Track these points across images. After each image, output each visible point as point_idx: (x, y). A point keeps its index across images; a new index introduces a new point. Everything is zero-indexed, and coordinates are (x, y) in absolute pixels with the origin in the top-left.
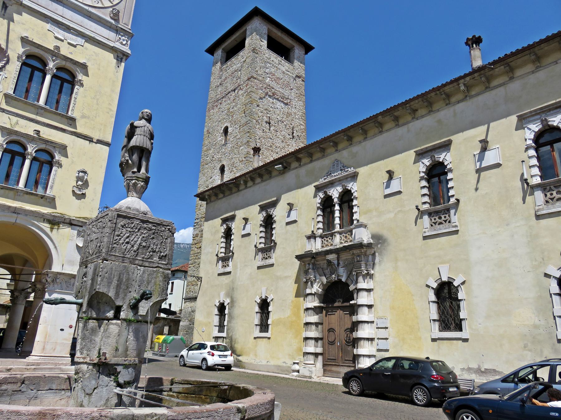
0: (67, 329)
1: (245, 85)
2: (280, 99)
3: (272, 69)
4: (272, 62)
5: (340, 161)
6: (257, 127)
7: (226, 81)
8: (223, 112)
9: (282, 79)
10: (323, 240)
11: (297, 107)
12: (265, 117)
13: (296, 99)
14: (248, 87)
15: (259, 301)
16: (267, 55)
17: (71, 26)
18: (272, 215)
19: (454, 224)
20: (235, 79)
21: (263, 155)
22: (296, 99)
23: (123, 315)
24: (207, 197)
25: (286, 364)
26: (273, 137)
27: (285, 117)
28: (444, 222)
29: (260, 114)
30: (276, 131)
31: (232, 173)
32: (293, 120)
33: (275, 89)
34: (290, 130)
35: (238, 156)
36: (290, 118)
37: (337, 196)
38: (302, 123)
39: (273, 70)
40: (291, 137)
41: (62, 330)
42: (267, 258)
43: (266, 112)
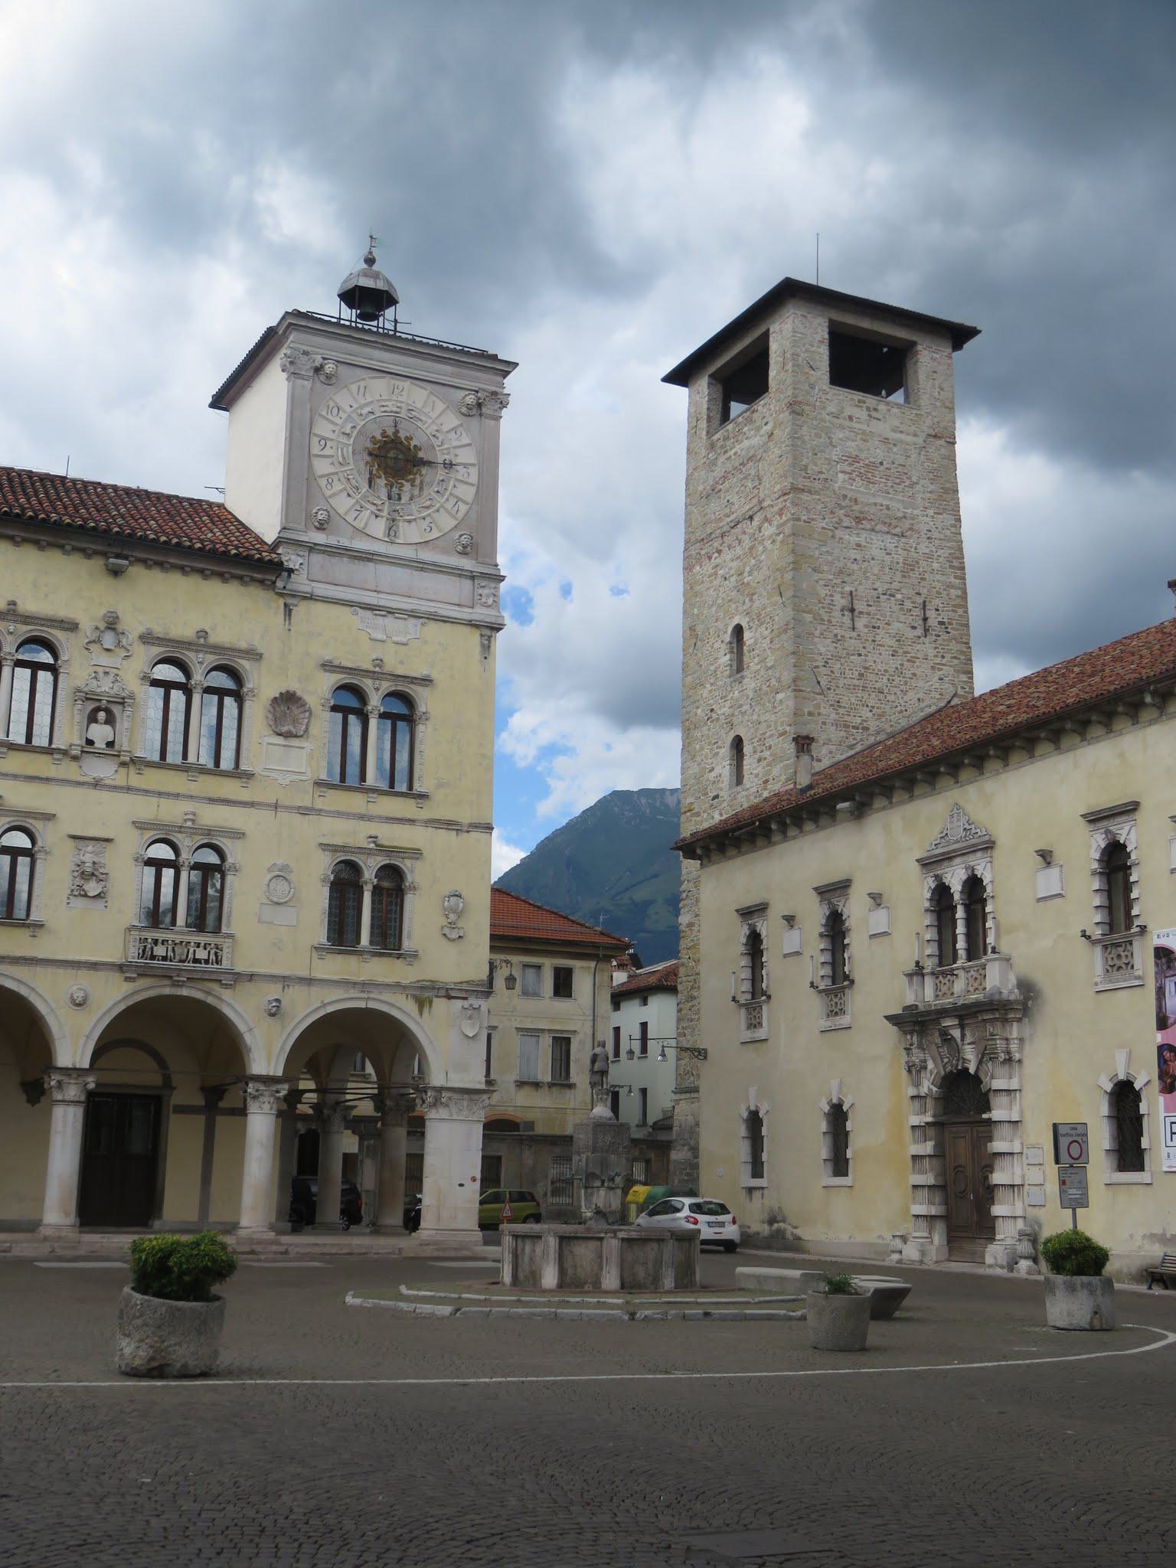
0: (468, 1184)
1: (776, 509)
2: (879, 527)
3: (849, 443)
4: (847, 423)
5: (963, 810)
6: (817, 633)
7: (727, 485)
8: (725, 579)
9: (881, 463)
10: (937, 981)
11: (935, 534)
12: (837, 597)
13: (931, 512)
14: (784, 518)
15: (826, 1108)
16: (831, 408)
17: (394, 605)
18: (841, 915)
19: (1137, 973)
20: (750, 485)
21: (840, 707)
22: (931, 512)
23: (606, 1184)
24: (699, 851)
25: (883, 1239)
26: (864, 648)
27: (898, 577)
28: (1124, 966)
29: (823, 592)
30: (874, 627)
31: (763, 763)
32: (924, 579)
33: (863, 502)
34: (918, 612)
35: (773, 718)
36: (915, 575)
37: (959, 888)
38: (953, 580)
39: (852, 447)
40: (919, 632)
41: (461, 1185)
42: (836, 1013)
43: (839, 581)
